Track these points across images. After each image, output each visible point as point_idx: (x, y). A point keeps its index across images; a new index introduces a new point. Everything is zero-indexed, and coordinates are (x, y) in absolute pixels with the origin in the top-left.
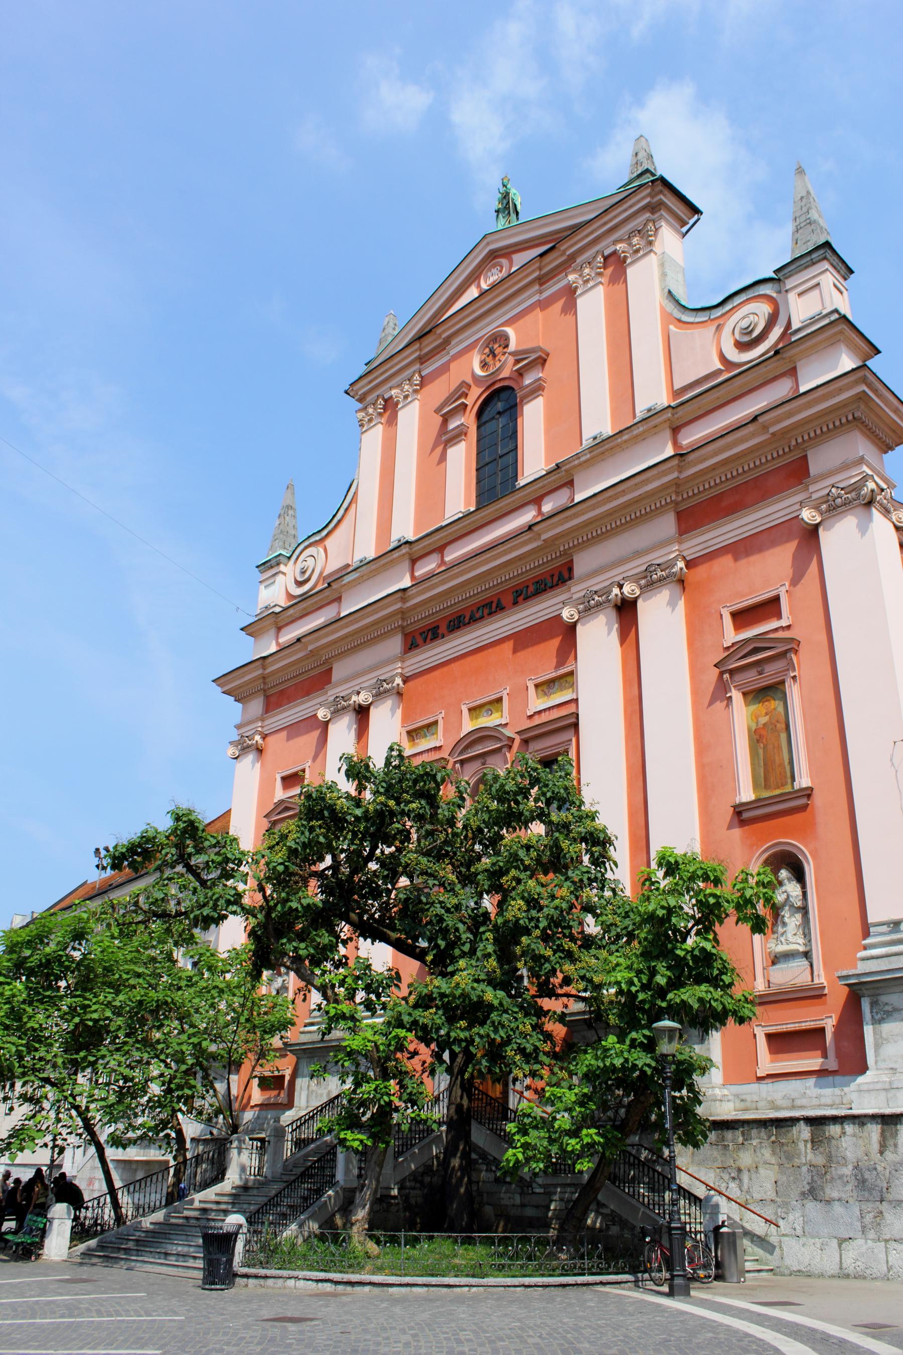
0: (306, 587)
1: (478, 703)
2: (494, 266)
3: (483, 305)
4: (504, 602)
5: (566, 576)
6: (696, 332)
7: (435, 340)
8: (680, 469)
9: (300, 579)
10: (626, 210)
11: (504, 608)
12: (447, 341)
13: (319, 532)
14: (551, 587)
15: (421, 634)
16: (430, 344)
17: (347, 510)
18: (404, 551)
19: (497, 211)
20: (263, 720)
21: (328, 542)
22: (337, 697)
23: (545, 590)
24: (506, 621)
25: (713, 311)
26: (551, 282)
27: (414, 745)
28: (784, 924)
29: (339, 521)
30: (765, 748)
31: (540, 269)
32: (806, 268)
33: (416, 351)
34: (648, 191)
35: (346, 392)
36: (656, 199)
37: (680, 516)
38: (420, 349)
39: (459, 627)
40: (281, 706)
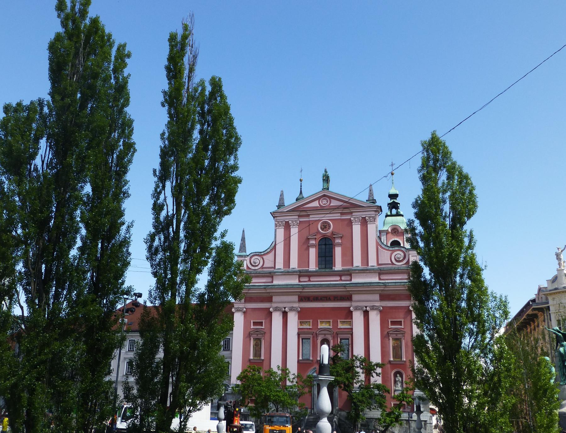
0: (256, 268)
1: (323, 321)
2: (325, 199)
8: (384, 288)
9: (253, 264)
11: (330, 300)
12: (308, 216)
15: (304, 298)
19: (324, 180)
21: (264, 257)
24: (332, 304)
27: (301, 325)
28: (398, 384)
31: (342, 211)
35: (271, 213)
36: (377, 210)
38: (300, 213)
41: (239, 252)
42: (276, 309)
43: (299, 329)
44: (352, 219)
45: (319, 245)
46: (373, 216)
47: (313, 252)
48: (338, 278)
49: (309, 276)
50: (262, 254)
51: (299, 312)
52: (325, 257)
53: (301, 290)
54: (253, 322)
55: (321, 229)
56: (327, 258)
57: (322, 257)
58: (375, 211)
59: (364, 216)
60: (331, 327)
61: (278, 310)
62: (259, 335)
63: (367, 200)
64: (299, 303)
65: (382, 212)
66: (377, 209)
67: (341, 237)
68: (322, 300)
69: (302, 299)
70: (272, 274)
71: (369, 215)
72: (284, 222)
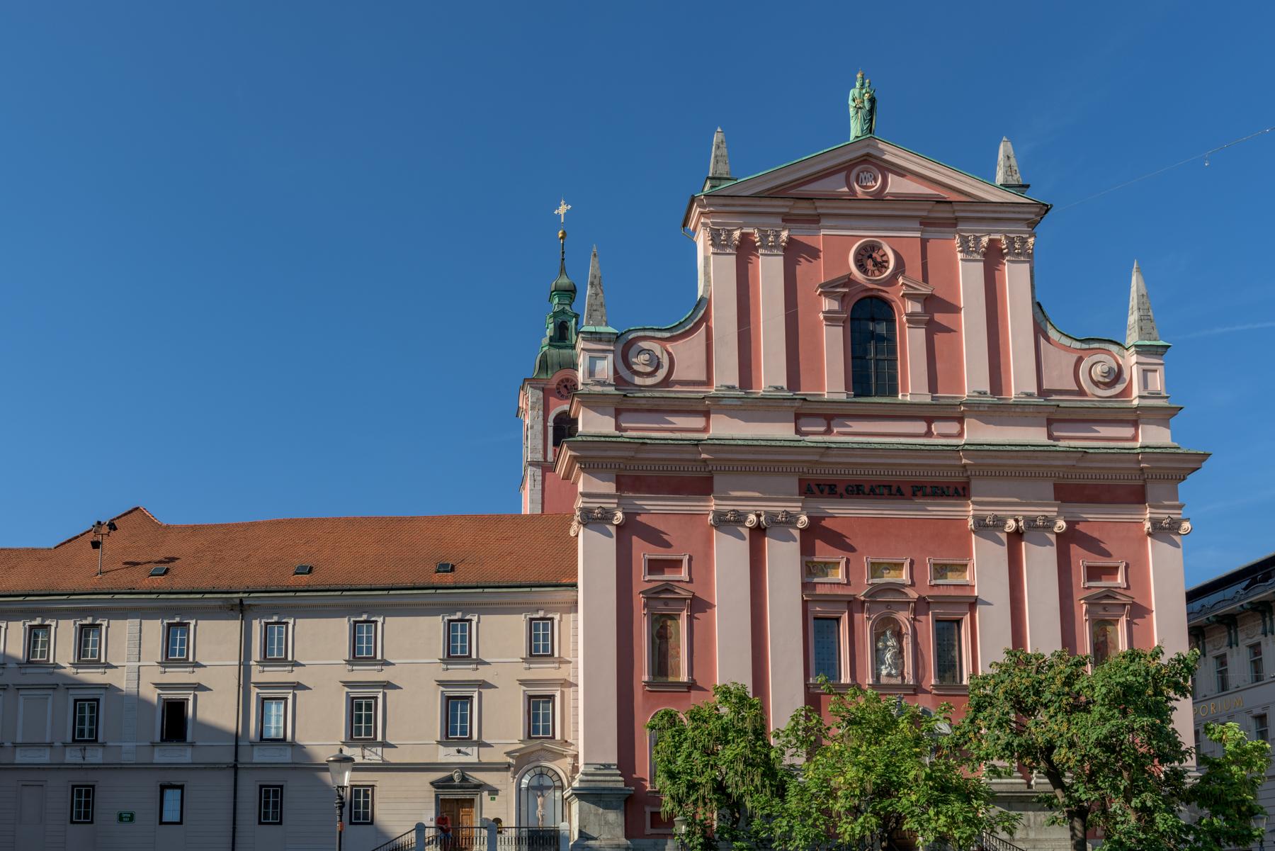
3: (868, 209)
4: (904, 490)
5: (961, 491)
6: (1063, 352)
10: (1014, 212)
11: (903, 495)
14: (949, 496)
15: (818, 485)
16: (803, 209)
18: (796, 404)
22: (734, 510)
23: (942, 496)
25: (1074, 342)
26: (933, 229)
29: (686, 331)
30: (1101, 655)
32: (1152, 354)
33: (787, 206)
37: (1056, 487)
38: (790, 209)
39: (858, 494)
43: (805, 586)
48: (921, 427)
50: (667, 335)
55: (861, 265)
62: (673, 606)
69: (814, 488)
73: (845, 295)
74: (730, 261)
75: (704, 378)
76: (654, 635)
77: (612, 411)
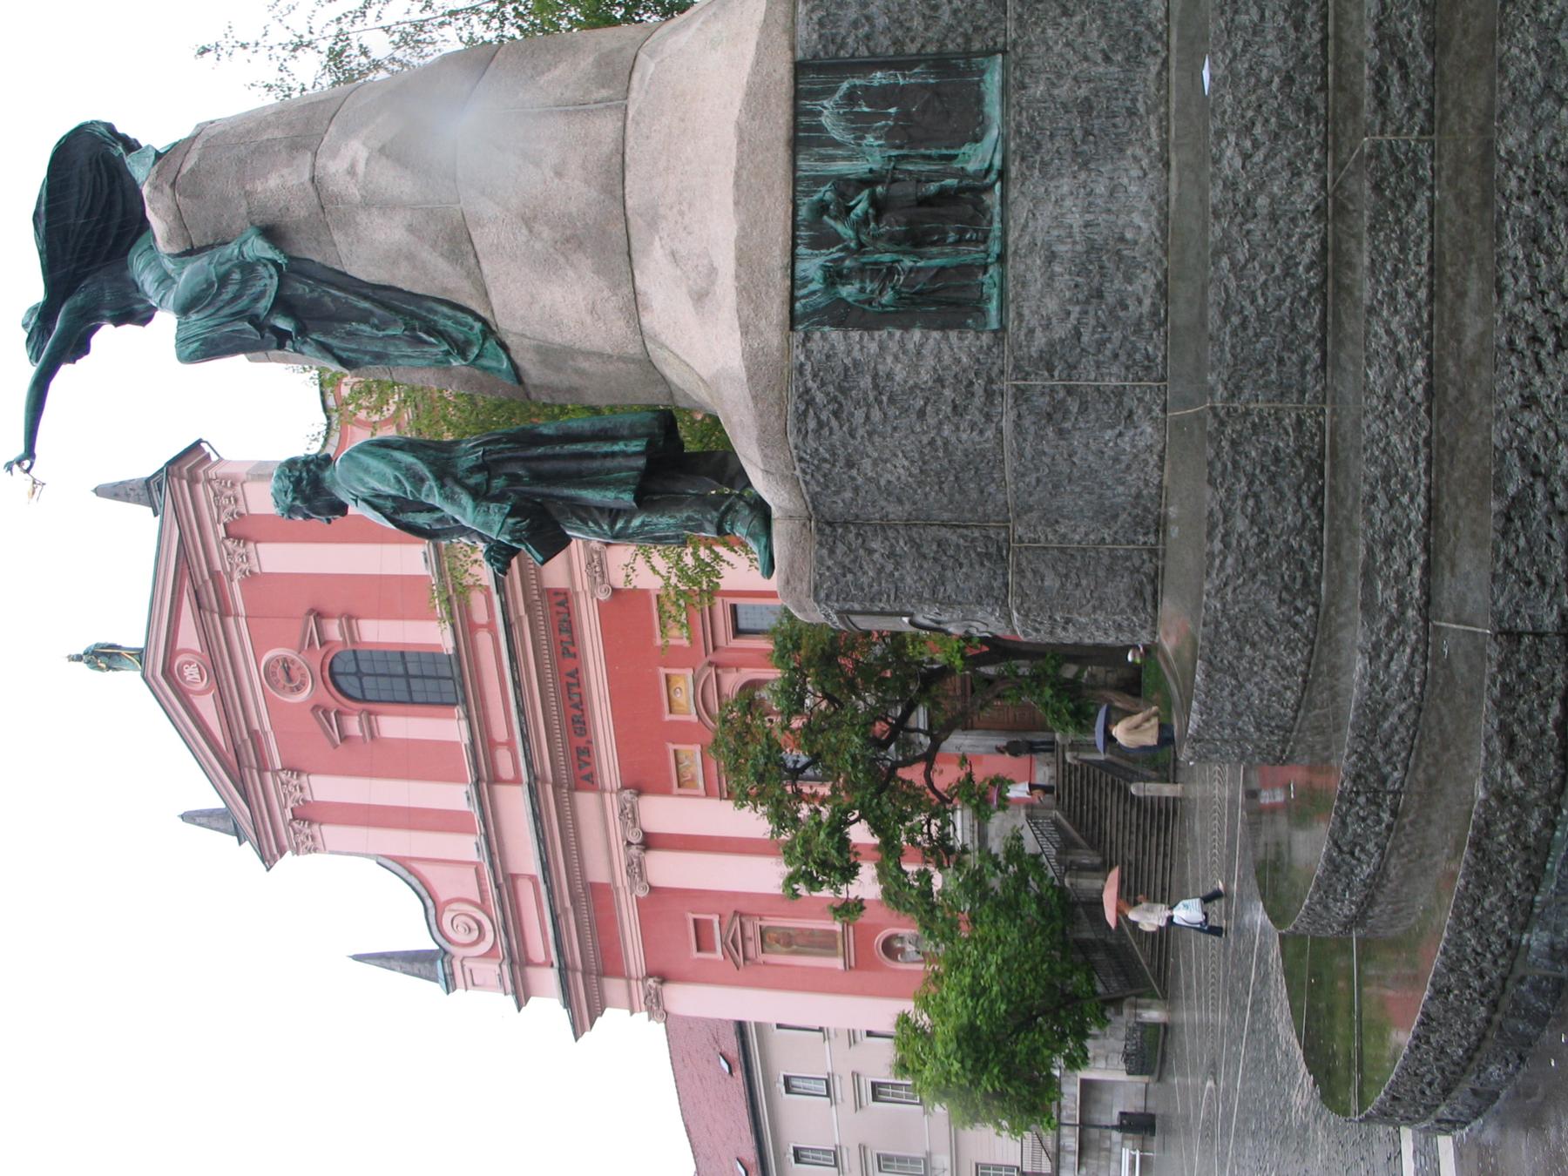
4: (569, 670)
5: (561, 598)
7: (246, 747)
9: (475, 934)
11: (577, 671)
12: (253, 735)
13: (426, 910)
14: (569, 613)
17: (411, 872)
19: (109, 668)
20: (629, 978)
21: (443, 896)
27: (693, 780)
29: (422, 883)
31: (212, 611)
34: (175, 480)
35: (268, 870)
38: (251, 767)
39: (584, 723)
40: (619, 954)
41: (437, 981)
42: (636, 870)
43: (708, 793)
44: (237, 576)
45: (364, 700)
46: (212, 495)
47: (396, 726)
48: (484, 639)
49: (491, 745)
50: (429, 903)
51: (640, 791)
52: (407, 676)
53: (549, 788)
54: (699, 949)
55: (298, 689)
56: (413, 669)
57: (410, 692)
58: (193, 481)
59: (221, 528)
60: (689, 672)
61: (640, 865)
62: (749, 932)
63: (156, 514)
64: (603, 790)
65: (200, 441)
66: (181, 478)
67: (319, 615)
68: (581, 703)
69: (583, 775)
70: (501, 880)
71: (210, 508)
72: (294, 824)
73: (338, 713)
74: (330, 832)
75: (472, 871)
76: (784, 949)
77: (531, 971)
